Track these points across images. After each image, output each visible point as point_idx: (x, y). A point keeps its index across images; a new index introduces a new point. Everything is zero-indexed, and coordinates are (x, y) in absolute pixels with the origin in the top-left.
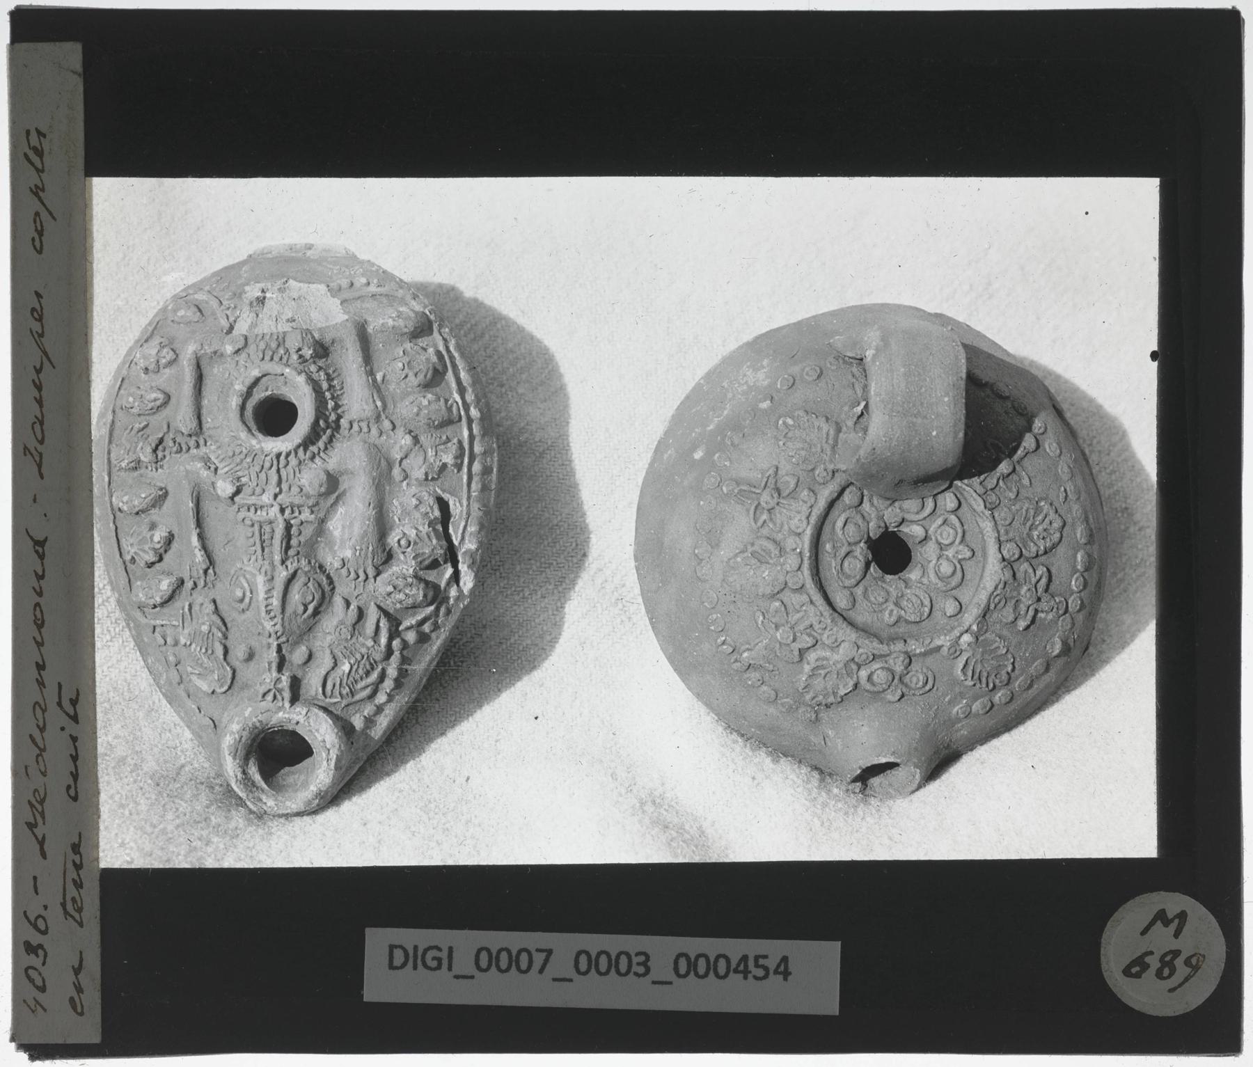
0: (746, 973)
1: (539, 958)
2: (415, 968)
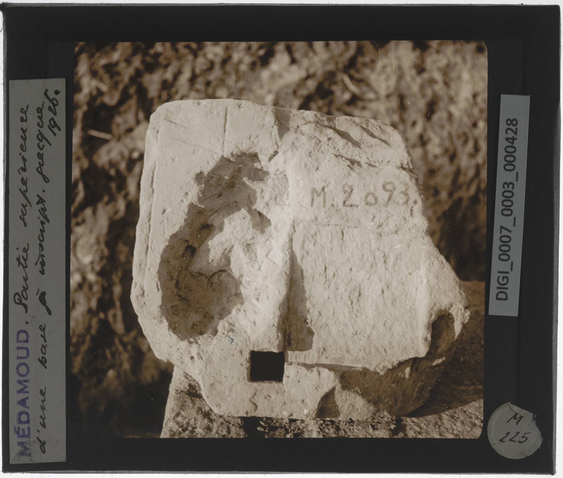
0: (514, 139)
1: (505, 232)
2: (507, 288)
